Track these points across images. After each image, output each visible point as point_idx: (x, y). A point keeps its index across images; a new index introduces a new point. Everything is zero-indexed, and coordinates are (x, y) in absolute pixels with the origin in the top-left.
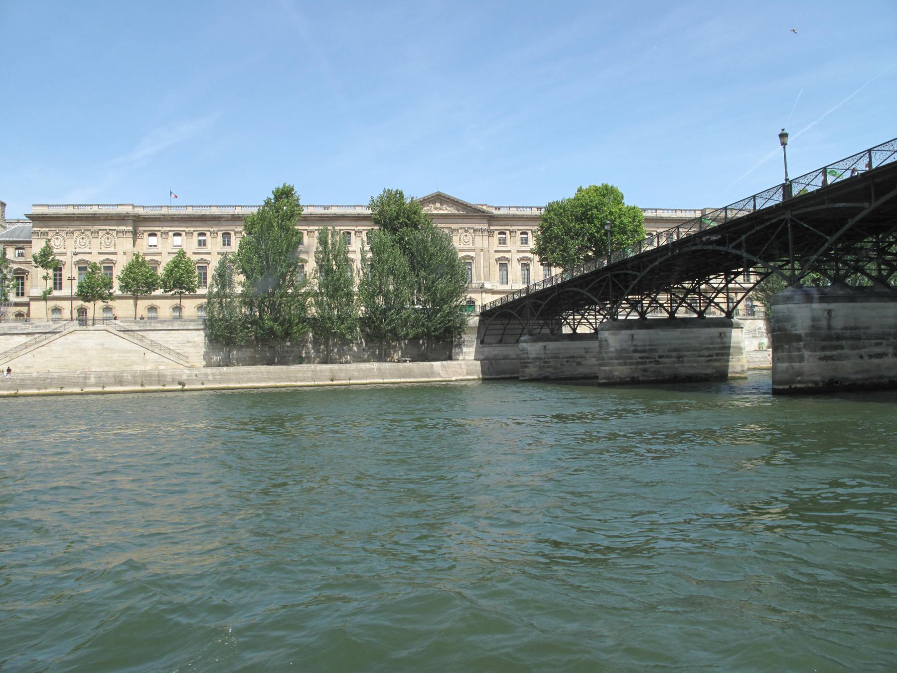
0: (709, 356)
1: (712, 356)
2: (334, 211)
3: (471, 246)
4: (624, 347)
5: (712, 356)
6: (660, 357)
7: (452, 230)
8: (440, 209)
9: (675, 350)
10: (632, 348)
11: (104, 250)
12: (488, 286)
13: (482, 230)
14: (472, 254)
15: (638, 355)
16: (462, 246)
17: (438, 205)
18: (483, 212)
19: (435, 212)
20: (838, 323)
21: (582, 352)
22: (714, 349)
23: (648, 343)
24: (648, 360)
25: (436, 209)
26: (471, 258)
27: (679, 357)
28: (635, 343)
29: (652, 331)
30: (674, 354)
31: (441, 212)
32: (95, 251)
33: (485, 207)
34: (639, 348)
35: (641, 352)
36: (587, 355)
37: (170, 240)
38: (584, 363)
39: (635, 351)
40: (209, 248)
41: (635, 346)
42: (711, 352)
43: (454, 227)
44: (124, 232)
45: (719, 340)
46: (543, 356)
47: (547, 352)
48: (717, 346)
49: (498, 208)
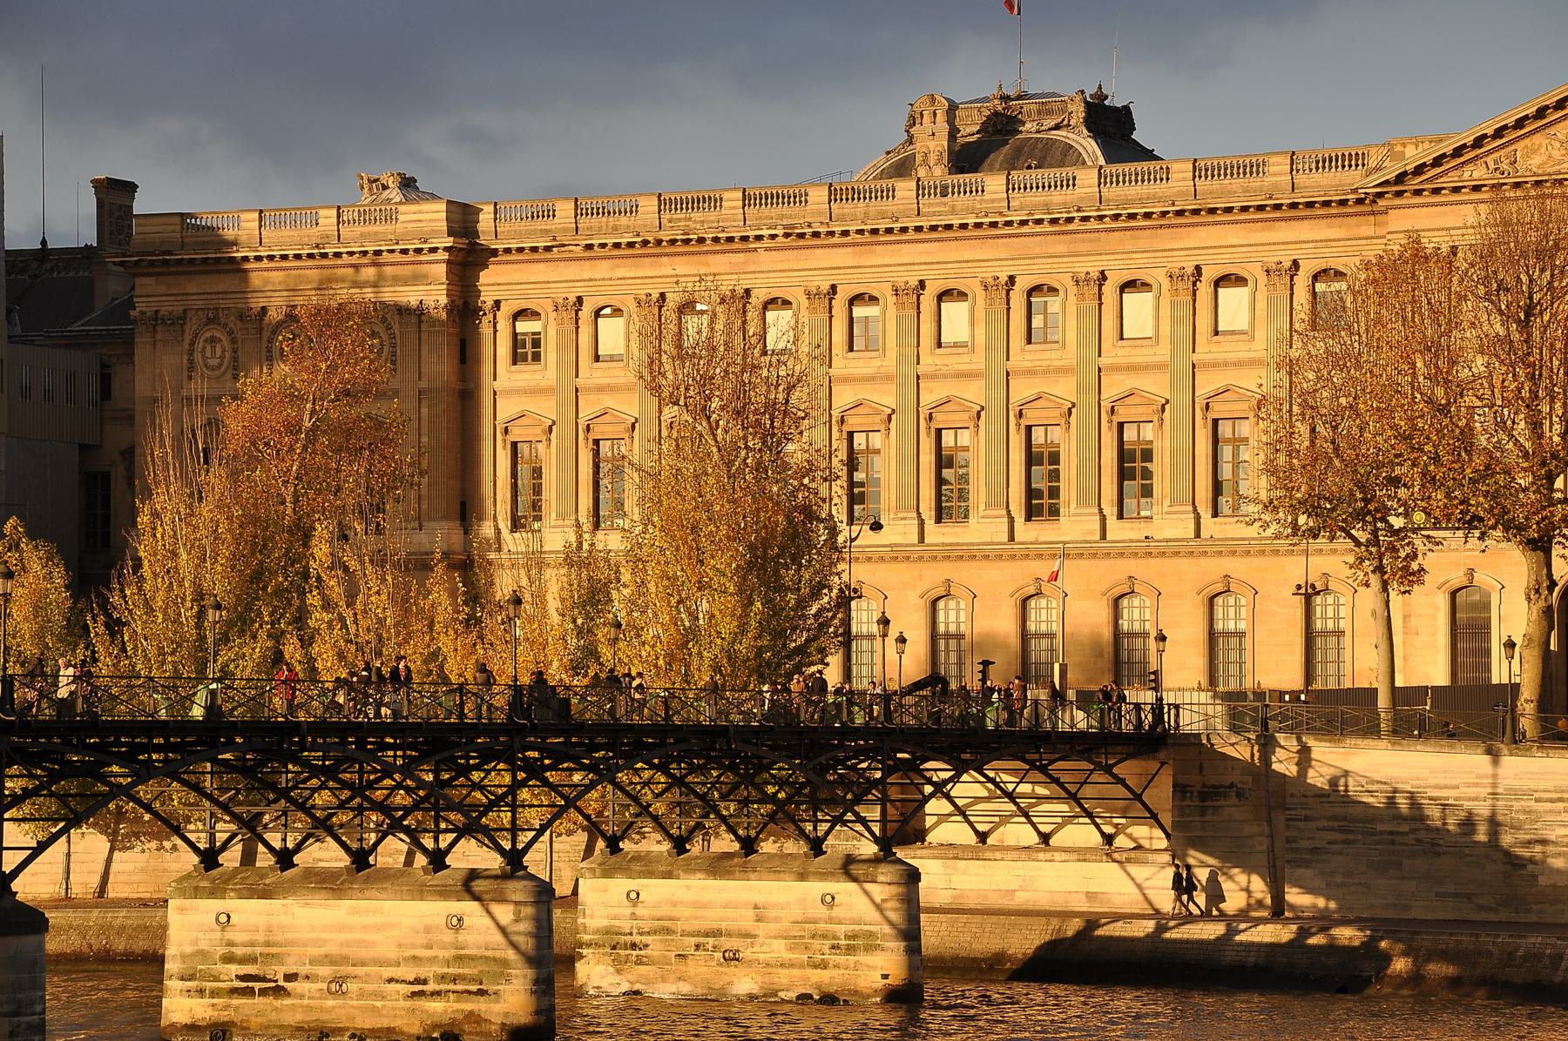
0: (417, 981)
1: (425, 982)
4: (204, 945)
5: (425, 982)
6: (291, 977)
9: (330, 960)
10: (221, 950)
15: (235, 969)
21: (746, 921)
22: (433, 960)
23: (261, 937)
24: (257, 986)
27: (340, 980)
28: (230, 935)
29: (275, 904)
30: (325, 971)
34: (239, 951)
35: (243, 961)
36: (761, 929)
38: (745, 954)
39: (229, 959)
41: (231, 944)
42: (422, 972)
45: (448, 936)
46: (626, 925)
47: (639, 911)
48: (441, 953)
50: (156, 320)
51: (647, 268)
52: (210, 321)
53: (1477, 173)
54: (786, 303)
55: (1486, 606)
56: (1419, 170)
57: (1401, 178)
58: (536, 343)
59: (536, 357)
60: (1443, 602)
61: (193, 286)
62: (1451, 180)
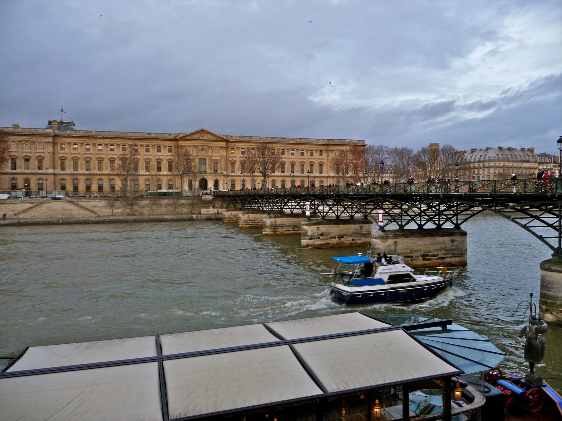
2: (153, 136)
3: (218, 155)
7: (210, 147)
11: (38, 151)
12: (225, 173)
13: (223, 147)
14: (218, 158)
16: (213, 155)
17: (203, 135)
19: (201, 138)
20: (278, 223)
31: (204, 138)
32: (33, 151)
37: (72, 147)
40: (92, 151)
43: (210, 145)
44: (48, 142)
49: (231, 136)
52: (13, 142)
53: (189, 138)
54: (101, 145)
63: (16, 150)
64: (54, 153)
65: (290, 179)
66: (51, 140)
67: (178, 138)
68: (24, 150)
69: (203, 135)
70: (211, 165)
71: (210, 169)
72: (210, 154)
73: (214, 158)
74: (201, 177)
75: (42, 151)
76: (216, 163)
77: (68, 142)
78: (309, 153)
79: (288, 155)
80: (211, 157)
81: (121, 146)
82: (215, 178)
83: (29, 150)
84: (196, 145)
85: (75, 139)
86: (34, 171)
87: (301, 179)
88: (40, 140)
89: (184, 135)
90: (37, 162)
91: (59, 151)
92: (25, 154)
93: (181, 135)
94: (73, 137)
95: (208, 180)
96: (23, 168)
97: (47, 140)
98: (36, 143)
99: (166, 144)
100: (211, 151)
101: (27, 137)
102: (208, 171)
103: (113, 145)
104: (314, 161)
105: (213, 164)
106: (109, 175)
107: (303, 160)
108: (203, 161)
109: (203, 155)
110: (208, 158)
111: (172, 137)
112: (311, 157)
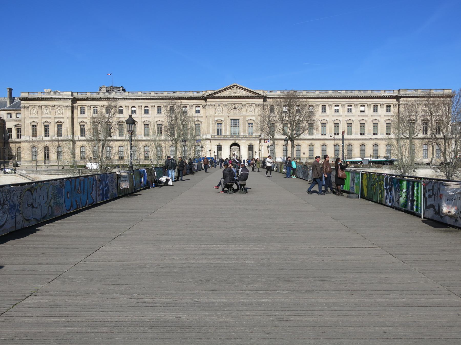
8: (236, 93)
11: (57, 116)
18: (260, 94)
19: (233, 95)
25: (234, 93)
26: (253, 120)
33: (261, 92)
43: (244, 103)
44: (67, 106)
50: (24, 107)
51: (101, 102)
55: (221, 147)
56: (212, 94)
57: (209, 95)
58: (84, 111)
59: (84, 113)
60: (216, 147)
61: (30, 102)
62: (215, 96)
63: (36, 116)
64: (73, 118)
65: (333, 142)
66: (69, 103)
67: (205, 96)
68: (44, 116)
69: (235, 91)
70: (244, 126)
71: (244, 131)
72: (244, 113)
73: (249, 118)
74: (232, 142)
75: (61, 116)
76: (251, 124)
77: (88, 105)
78: (372, 109)
79: (343, 112)
80: (244, 117)
81: (143, 108)
82: (249, 142)
83: (49, 116)
84: (226, 103)
85: (94, 102)
86: (28, 139)
87: (361, 142)
88: (59, 104)
89: (212, 92)
90: (56, 129)
91: (80, 115)
92: (44, 120)
93: (210, 92)
94: (93, 100)
95: (240, 145)
96: (43, 135)
97: (66, 105)
98: (55, 107)
99: (192, 104)
100: (244, 109)
101: (47, 102)
102: (242, 134)
103: (135, 107)
104: (378, 118)
105: (247, 125)
106: (155, 140)
107: (364, 118)
108: (235, 123)
109: (235, 114)
110: (241, 119)
111: (200, 95)
112: (375, 114)
